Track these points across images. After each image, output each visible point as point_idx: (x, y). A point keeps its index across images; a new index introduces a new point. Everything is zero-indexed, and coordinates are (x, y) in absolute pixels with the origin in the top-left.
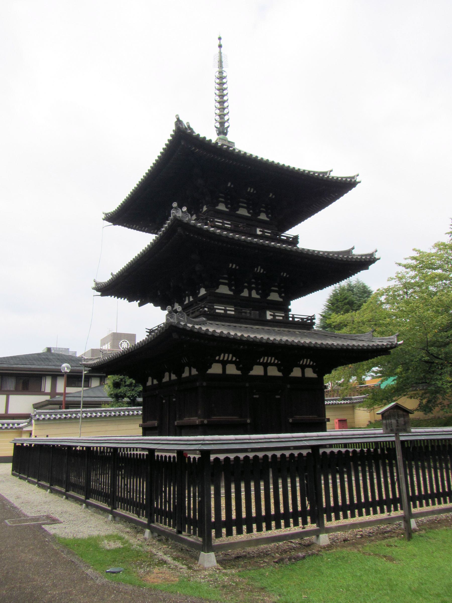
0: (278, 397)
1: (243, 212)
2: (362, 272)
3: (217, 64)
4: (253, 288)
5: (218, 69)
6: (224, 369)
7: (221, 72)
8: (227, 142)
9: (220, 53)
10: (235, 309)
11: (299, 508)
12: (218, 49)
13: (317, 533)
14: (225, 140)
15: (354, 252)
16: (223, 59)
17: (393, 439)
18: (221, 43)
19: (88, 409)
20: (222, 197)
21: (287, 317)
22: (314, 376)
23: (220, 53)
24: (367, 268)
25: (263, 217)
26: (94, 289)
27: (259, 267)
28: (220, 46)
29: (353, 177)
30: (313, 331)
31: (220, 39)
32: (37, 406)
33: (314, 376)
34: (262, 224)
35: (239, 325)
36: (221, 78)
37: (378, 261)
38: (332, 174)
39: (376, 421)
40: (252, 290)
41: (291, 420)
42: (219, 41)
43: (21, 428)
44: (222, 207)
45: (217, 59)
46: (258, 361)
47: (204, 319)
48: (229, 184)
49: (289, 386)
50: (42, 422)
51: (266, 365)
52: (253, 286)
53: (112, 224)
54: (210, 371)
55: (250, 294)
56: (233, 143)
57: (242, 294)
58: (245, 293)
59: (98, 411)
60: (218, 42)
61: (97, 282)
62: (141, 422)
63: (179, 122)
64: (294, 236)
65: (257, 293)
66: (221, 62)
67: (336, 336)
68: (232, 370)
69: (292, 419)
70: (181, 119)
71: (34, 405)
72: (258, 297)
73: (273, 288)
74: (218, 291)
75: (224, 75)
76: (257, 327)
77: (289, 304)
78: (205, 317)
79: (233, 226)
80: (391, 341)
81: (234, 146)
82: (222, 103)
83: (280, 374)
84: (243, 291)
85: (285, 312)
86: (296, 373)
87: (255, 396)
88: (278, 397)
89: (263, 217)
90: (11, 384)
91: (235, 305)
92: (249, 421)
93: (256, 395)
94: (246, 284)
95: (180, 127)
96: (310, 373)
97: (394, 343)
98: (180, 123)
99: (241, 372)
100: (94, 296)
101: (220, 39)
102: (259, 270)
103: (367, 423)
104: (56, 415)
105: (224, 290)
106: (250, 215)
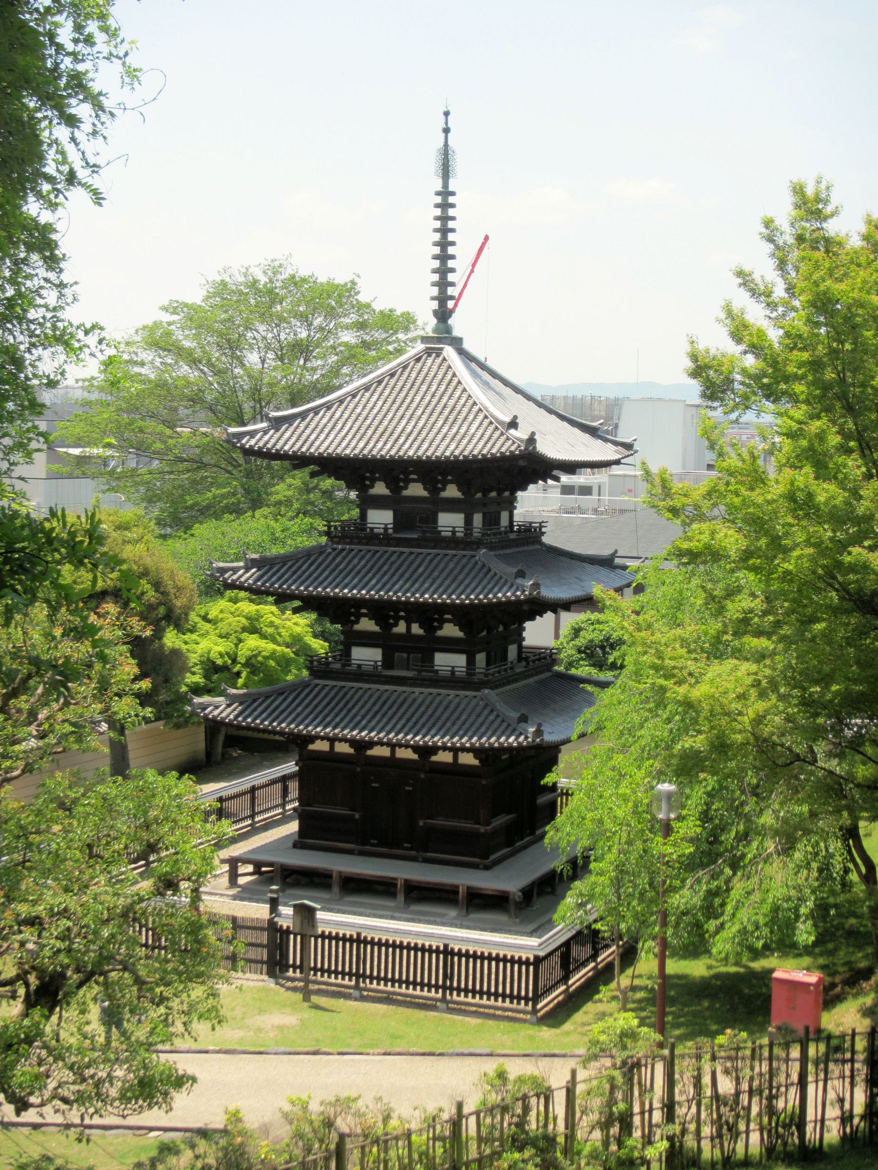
0: (407, 788)
5: (438, 186)
9: (446, 145)
23: (446, 145)
28: (446, 131)
31: (447, 114)
41: (421, 823)
55: (409, 628)
57: (396, 630)
58: (401, 628)
65: (421, 627)
73: (446, 616)
84: (396, 625)
88: (407, 788)
92: (357, 816)
94: (402, 614)
101: (447, 114)
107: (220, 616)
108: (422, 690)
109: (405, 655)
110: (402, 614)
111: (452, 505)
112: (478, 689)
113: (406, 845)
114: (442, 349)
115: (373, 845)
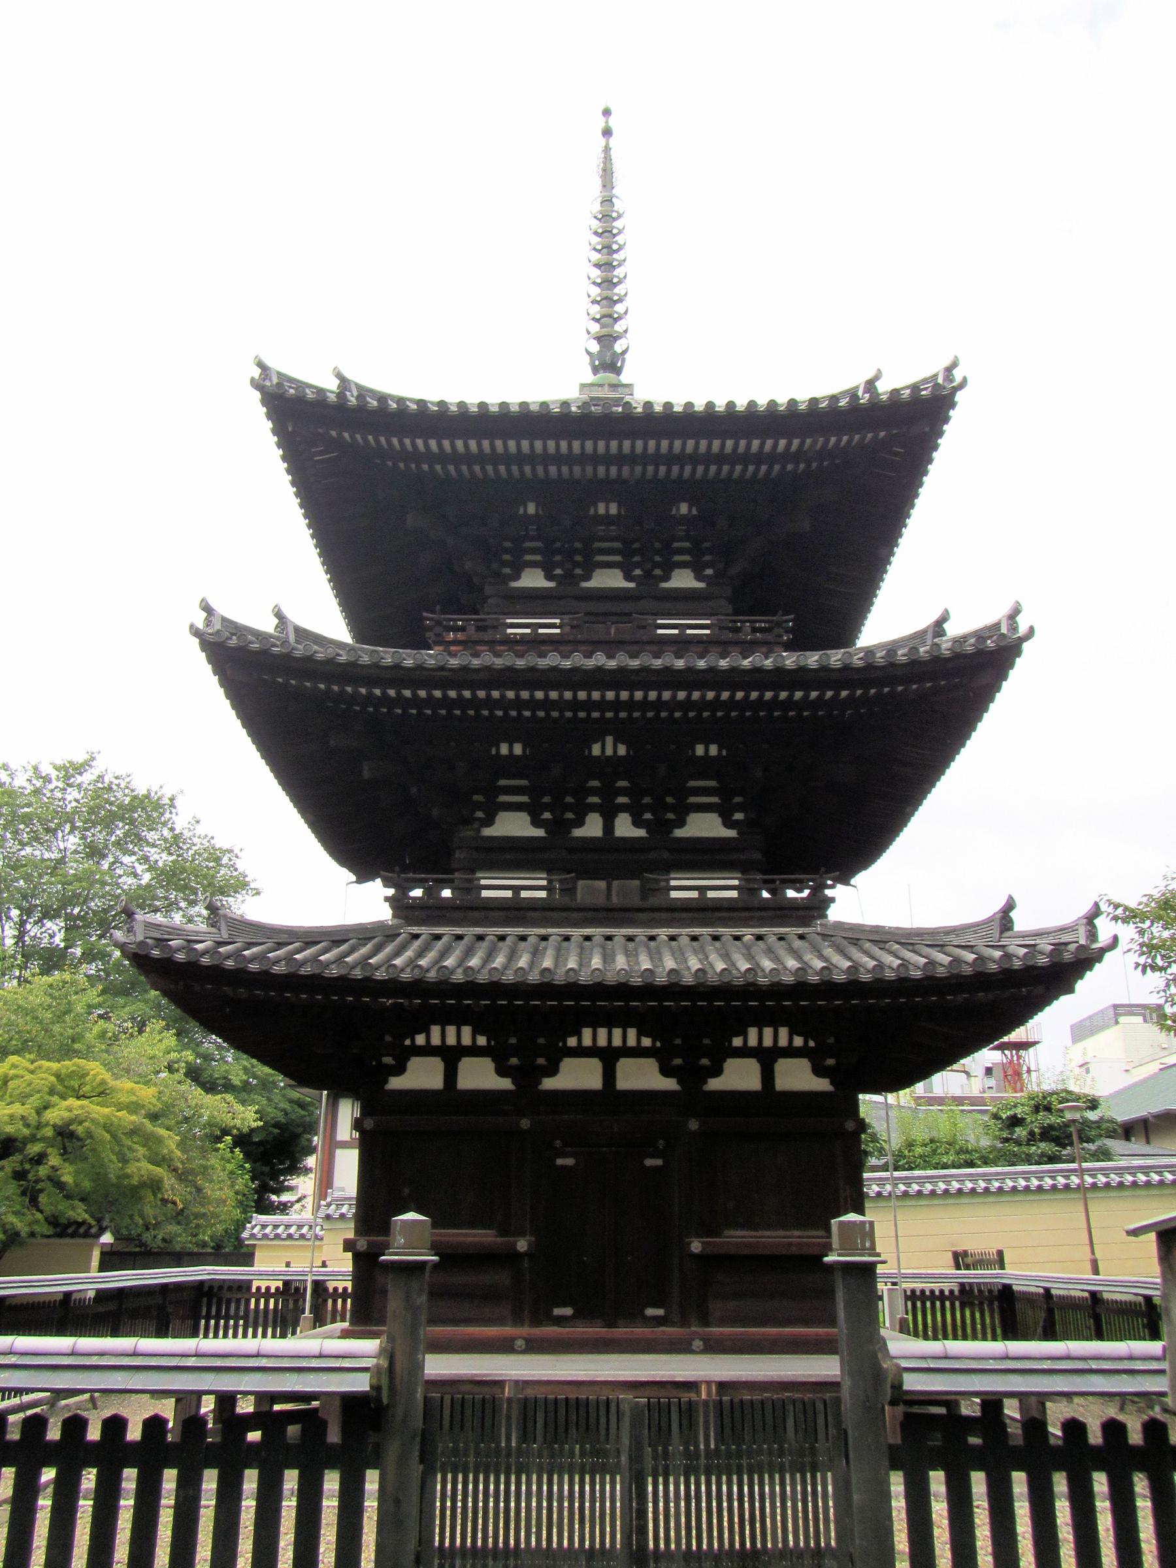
0: (649, 1162)
1: (610, 579)
3: (597, 182)
4: (623, 808)
7: (608, 201)
8: (606, 388)
9: (607, 149)
10: (550, 881)
16: (617, 166)
18: (611, 124)
20: (533, 551)
22: (822, 1085)
23: (607, 149)
27: (609, 740)
28: (607, 132)
31: (607, 113)
33: (822, 1085)
34: (684, 602)
35: (520, 931)
37: (1026, 646)
38: (884, 387)
40: (615, 816)
42: (603, 119)
44: (533, 579)
46: (561, 1044)
49: (693, 1125)
52: (622, 800)
55: (609, 827)
57: (578, 833)
58: (592, 827)
60: (601, 122)
65: (637, 823)
66: (607, 174)
67: (884, 938)
69: (703, 1243)
72: (641, 833)
75: (618, 205)
79: (567, 629)
80: (1065, 938)
82: (608, 283)
83: (669, 1084)
84: (580, 823)
85: (743, 873)
87: (560, 1162)
88: (649, 1162)
89: (683, 580)
91: (549, 868)
92: (522, 1245)
93: (564, 1155)
94: (594, 800)
99: (513, 1083)
101: (607, 113)
102: (607, 748)
107: (12, 1072)
108: (673, 931)
109: (602, 884)
110: (594, 800)
112: (805, 921)
113: (650, 1312)
115: (560, 1321)
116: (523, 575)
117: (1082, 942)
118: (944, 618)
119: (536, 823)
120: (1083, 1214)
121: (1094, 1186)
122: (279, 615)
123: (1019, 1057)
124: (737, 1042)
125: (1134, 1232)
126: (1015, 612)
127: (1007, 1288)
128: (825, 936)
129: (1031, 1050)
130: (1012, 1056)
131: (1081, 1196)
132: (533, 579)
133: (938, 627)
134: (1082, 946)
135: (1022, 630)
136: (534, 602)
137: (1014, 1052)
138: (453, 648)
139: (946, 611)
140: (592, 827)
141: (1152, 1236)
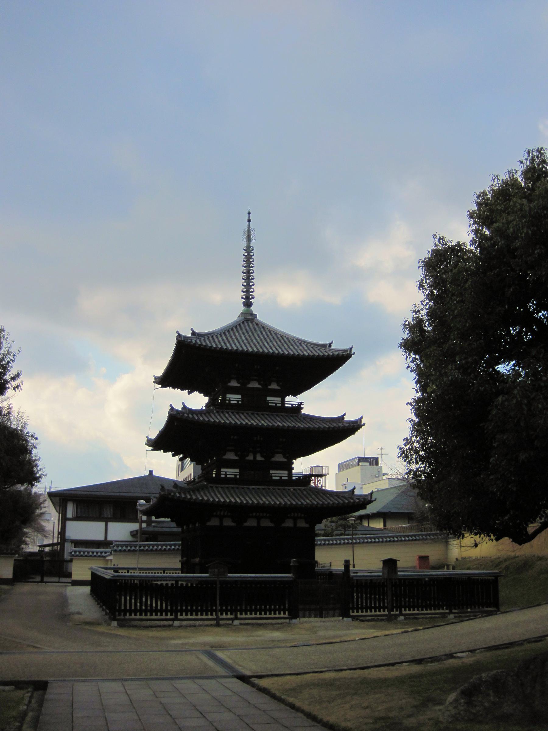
1: (254, 385)
2: (352, 435)
5: (246, 244)
6: (221, 522)
7: (249, 247)
8: (249, 315)
9: (249, 227)
11: (159, 608)
12: (247, 223)
13: (173, 620)
14: (247, 314)
15: (346, 418)
17: (216, 579)
19: (159, 543)
21: (290, 474)
23: (249, 227)
24: (354, 433)
25: (274, 386)
26: (146, 444)
28: (249, 221)
29: (346, 350)
30: (308, 488)
31: (249, 213)
32: (133, 534)
36: (249, 251)
37: (363, 427)
39: (462, 558)
43: (105, 557)
44: (234, 383)
45: (246, 235)
47: (206, 483)
48: (237, 365)
50: (118, 553)
51: (259, 519)
53: (160, 386)
54: (209, 524)
55: (255, 457)
56: (256, 315)
57: (247, 458)
58: (250, 457)
59: (169, 544)
61: (149, 439)
62: (180, 559)
63: (179, 335)
64: (299, 403)
65: (262, 456)
68: (228, 522)
70: (181, 333)
71: (131, 532)
72: (262, 459)
74: (225, 457)
76: (253, 487)
77: (293, 463)
78: (206, 482)
81: (256, 318)
84: (248, 456)
86: (288, 523)
89: (274, 386)
90: (108, 512)
95: (180, 340)
96: (302, 524)
97: (367, 500)
98: (179, 337)
100: (147, 450)
101: (249, 213)
103: (455, 560)
104: (131, 547)
105: (231, 456)
106: (260, 387)
111: (274, 393)
114: (253, 319)
116: (231, 381)
117: (369, 499)
118: (345, 415)
119: (236, 455)
120: (352, 552)
121: (356, 543)
122: (183, 403)
123: (318, 481)
124: (289, 515)
125: (381, 561)
126: (362, 418)
127: (331, 572)
128: (310, 490)
129: (323, 477)
130: (315, 480)
131: (352, 546)
132: (234, 383)
133: (342, 417)
134: (369, 500)
135: (362, 423)
136: (234, 391)
137: (316, 478)
138: (217, 407)
139: (345, 413)
140: (250, 457)
141: (382, 562)
